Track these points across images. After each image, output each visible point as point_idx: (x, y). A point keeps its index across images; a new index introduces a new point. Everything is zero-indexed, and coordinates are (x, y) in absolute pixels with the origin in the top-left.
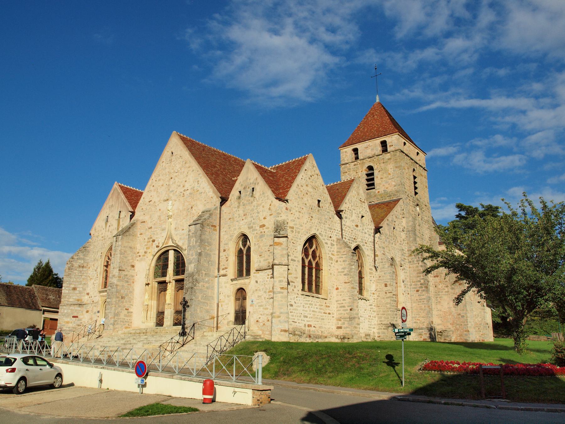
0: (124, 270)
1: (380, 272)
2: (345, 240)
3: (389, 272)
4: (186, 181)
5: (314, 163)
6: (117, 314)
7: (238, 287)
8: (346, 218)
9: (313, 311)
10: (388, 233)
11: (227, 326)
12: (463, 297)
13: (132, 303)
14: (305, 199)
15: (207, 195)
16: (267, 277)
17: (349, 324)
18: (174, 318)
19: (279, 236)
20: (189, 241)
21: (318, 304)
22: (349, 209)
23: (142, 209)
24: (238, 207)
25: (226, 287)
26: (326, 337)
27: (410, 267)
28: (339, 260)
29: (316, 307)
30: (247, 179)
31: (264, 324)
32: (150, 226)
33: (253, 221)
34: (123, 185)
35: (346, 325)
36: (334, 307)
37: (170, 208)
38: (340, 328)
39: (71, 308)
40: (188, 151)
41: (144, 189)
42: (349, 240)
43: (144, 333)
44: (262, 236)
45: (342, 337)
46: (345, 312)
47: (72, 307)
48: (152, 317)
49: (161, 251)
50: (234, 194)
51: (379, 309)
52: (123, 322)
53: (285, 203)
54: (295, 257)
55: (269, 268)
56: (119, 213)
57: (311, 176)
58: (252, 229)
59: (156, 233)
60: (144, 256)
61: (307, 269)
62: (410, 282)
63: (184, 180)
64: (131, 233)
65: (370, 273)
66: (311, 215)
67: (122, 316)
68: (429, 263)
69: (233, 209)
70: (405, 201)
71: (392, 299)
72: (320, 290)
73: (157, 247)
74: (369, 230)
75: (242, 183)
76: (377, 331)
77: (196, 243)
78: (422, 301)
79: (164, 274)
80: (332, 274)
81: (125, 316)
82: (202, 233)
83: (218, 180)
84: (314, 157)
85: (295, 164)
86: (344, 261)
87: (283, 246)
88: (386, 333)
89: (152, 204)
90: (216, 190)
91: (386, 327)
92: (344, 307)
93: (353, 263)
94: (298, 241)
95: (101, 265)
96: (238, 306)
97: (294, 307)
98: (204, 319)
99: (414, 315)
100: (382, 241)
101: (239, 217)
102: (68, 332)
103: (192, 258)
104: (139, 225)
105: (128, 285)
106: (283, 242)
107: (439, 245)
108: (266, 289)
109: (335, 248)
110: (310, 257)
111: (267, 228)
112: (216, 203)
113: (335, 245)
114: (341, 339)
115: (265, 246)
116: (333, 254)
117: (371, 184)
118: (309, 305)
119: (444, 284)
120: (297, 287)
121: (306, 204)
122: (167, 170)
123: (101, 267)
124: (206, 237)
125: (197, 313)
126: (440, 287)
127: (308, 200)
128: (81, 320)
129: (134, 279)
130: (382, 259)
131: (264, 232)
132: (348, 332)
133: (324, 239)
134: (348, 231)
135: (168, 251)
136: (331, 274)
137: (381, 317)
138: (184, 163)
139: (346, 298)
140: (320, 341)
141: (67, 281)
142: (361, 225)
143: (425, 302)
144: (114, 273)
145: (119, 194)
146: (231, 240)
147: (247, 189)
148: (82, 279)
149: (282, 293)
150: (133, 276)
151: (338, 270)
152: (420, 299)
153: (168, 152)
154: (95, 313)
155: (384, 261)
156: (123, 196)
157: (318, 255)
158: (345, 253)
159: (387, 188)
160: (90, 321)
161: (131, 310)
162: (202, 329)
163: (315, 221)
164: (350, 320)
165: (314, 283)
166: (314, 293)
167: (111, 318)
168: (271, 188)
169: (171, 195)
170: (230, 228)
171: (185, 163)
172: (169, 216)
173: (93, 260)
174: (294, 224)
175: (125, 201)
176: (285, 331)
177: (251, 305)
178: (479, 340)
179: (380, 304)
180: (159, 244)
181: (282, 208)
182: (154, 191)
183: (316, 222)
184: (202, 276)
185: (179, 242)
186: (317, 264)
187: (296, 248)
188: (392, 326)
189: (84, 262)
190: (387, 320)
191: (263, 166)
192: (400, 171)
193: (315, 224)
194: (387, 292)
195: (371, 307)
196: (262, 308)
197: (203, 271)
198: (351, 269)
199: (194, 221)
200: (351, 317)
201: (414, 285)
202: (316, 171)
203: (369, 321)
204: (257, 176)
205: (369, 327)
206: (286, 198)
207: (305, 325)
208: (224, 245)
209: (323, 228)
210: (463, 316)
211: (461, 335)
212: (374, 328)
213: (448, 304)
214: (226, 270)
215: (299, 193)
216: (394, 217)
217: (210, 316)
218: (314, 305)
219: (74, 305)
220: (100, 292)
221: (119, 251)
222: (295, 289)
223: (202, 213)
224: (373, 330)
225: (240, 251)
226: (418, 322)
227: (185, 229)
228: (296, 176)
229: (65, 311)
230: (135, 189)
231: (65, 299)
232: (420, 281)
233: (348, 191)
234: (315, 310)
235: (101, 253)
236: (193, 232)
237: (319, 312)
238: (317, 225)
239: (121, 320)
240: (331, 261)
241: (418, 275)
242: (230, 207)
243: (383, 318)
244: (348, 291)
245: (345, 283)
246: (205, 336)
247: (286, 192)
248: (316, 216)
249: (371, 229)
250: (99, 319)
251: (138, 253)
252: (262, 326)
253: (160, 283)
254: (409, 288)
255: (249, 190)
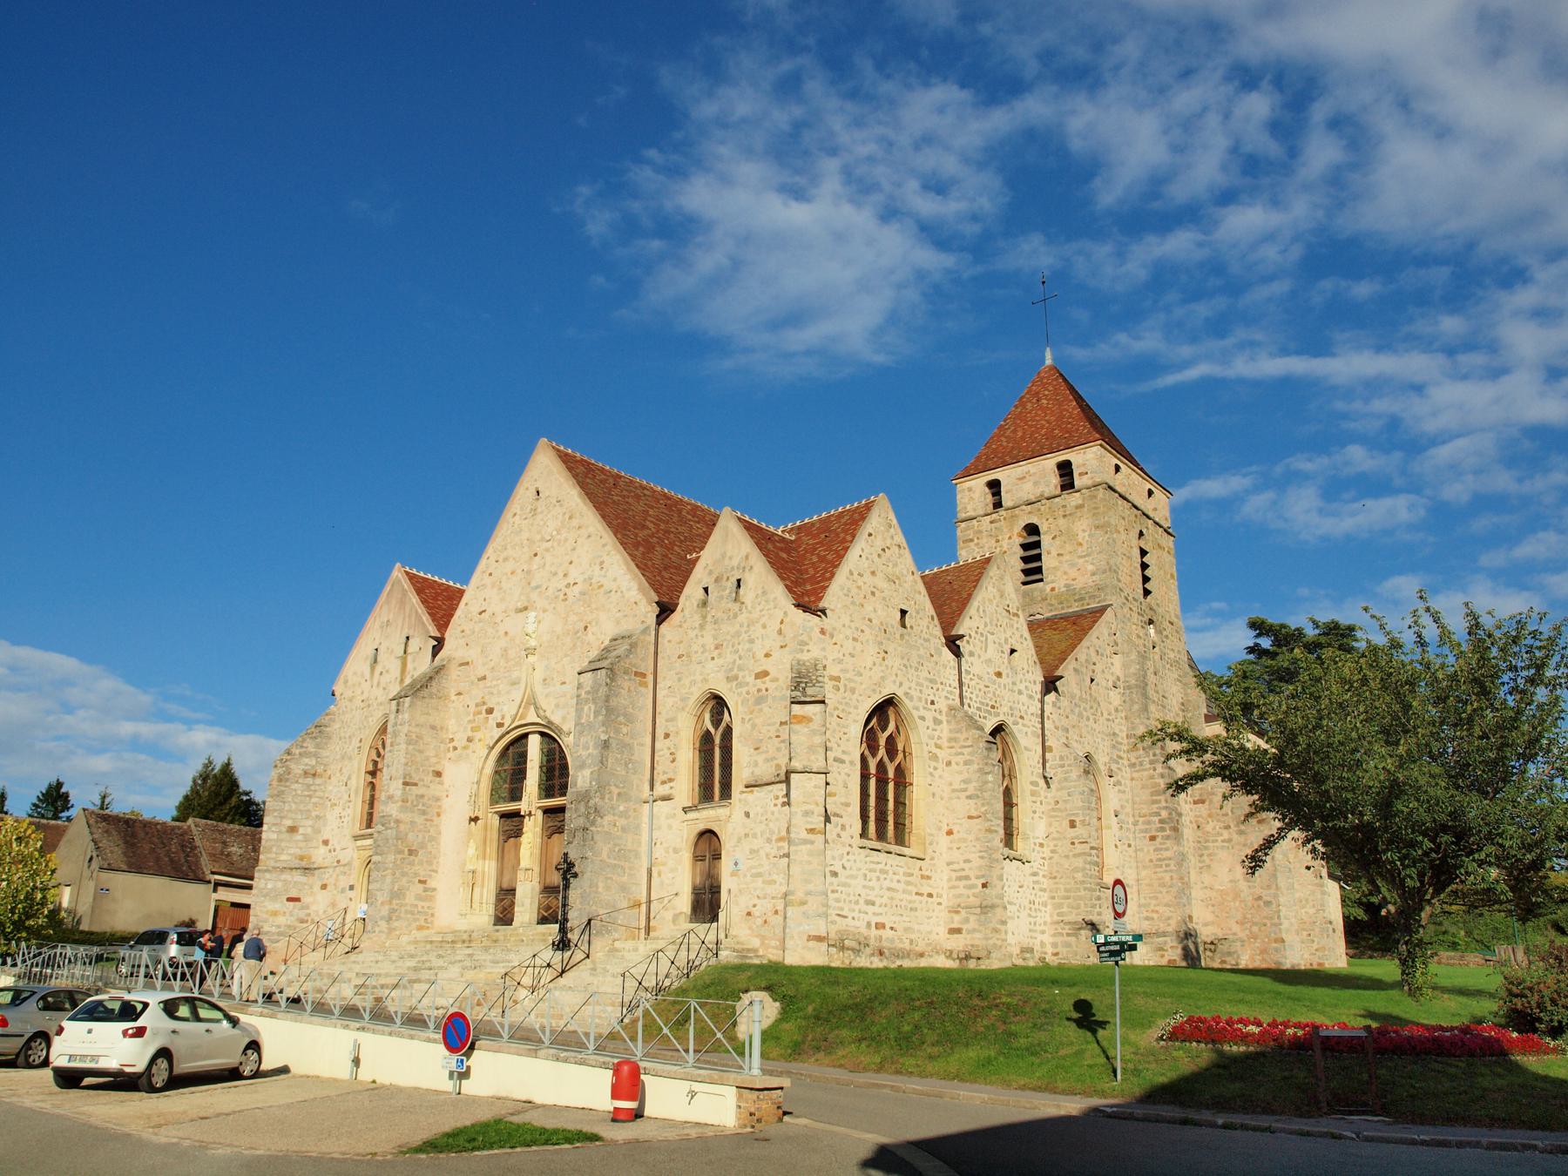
0: (416, 784)
1: (1058, 790)
2: (970, 711)
3: (1080, 790)
4: (571, 563)
5: (892, 516)
6: (397, 895)
7: (702, 827)
8: (971, 654)
9: (889, 889)
10: (1076, 691)
11: (672, 927)
12: (1266, 854)
13: (434, 867)
14: (869, 608)
15: (623, 597)
16: (774, 802)
17: (979, 920)
18: (540, 904)
19: (803, 699)
20: (579, 711)
21: (901, 871)
22: (980, 631)
23: (463, 631)
24: (702, 627)
25: (670, 827)
26: (922, 955)
27: (1132, 779)
28: (954, 760)
29: (897, 877)
30: (723, 556)
31: (765, 922)
32: (480, 674)
33: (738, 662)
34: (414, 571)
35: (972, 924)
36: (941, 880)
37: (530, 628)
38: (958, 931)
39: (283, 877)
40: (578, 488)
41: (466, 581)
42: (979, 709)
43: (464, 942)
44: (760, 700)
45: (962, 955)
46: (970, 892)
47: (286, 876)
48: (484, 901)
49: (508, 736)
50: (690, 595)
51: (1056, 883)
52: (413, 914)
53: (819, 616)
54: (844, 752)
55: (778, 779)
56: (404, 640)
57: (884, 550)
58: (735, 683)
59: (495, 692)
60: (465, 748)
61: (873, 782)
62: (1133, 816)
63: (568, 558)
64: (434, 690)
65: (1033, 794)
66: (883, 647)
67: (410, 898)
68: (1181, 768)
69: (690, 631)
70: (1119, 611)
71: (1089, 859)
72: (907, 835)
73: (500, 725)
74: (1027, 684)
75: (710, 567)
76: (1051, 940)
77: (595, 717)
78: (1164, 863)
79: (516, 795)
80: (937, 796)
81: (419, 897)
82: (610, 690)
83: (651, 560)
84: (892, 503)
85: (843, 521)
86: (966, 763)
87: (815, 725)
88: (1074, 944)
90: (647, 585)
91: (1074, 929)
92: (967, 878)
93: (988, 769)
94: (850, 713)
95: (359, 769)
96: (701, 875)
97: (841, 878)
98: (614, 906)
99: (1145, 898)
100: (1061, 711)
101: (702, 653)
102: (276, 937)
103: (584, 753)
104: (454, 672)
105: (427, 820)
106: (815, 715)
107: (1207, 722)
108: (772, 832)
109: (945, 730)
110: (882, 752)
111: (772, 681)
112: (646, 617)
113: (945, 722)
114: (961, 960)
115: (769, 725)
116: (937, 746)
117: (1032, 569)
118: (878, 874)
119: (1219, 821)
120: (847, 827)
121: (870, 620)
122: (525, 535)
123: (358, 777)
124: (621, 701)
125: (597, 892)
126: (1209, 828)
127: (875, 611)
128: (307, 907)
129: (440, 807)
130: (1061, 758)
131: (767, 690)
132: (977, 942)
133: (917, 709)
134: (978, 687)
135: (525, 736)
136: (934, 795)
137: (1060, 906)
138: (567, 516)
139: (971, 857)
140: (907, 963)
141: (275, 810)
142: (1009, 671)
143: (1172, 867)
144: (391, 792)
145: (404, 593)
146: (683, 709)
147: (724, 583)
148: (310, 807)
149: (812, 843)
150: (438, 799)
151: (951, 784)
152: (1160, 860)
153: (527, 489)
154: (343, 891)
155: (1066, 763)
156: (414, 599)
157: (900, 747)
158: (969, 743)
159: (1074, 580)
160: (330, 911)
161: (432, 884)
162: (609, 932)
163: (894, 662)
164: (982, 913)
165: (891, 819)
166: (890, 843)
167: (382, 903)
168: (782, 579)
169: (534, 596)
170: (679, 680)
171: (570, 518)
172: (528, 649)
173: (338, 757)
174: (842, 670)
175: (420, 611)
176: (819, 939)
177: (734, 874)
178: (1311, 965)
179: (1057, 872)
180: (503, 718)
181: (812, 629)
182: (493, 587)
183: (896, 664)
184: (611, 799)
185: (553, 712)
186: (900, 771)
187: (846, 731)
188: (1089, 927)
189: (317, 762)
190: (1075, 911)
191: (764, 526)
192: (1107, 536)
193: (895, 669)
194: (1076, 841)
195: (1035, 878)
196: (760, 879)
197: (613, 788)
198: (986, 782)
199: (590, 662)
200: (984, 903)
201: (1144, 823)
202: (896, 538)
203: (1030, 915)
204: (748, 550)
205: (1030, 931)
206: (821, 605)
207: (869, 924)
208: (667, 721)
209: (914, 678)
210: (1268, 903)
211: (1263, 951)
212: (1043, 932)
213: (1230, 871)
214: (671, 784)
215: (854, 591)
216: (1092, 651)
217: (629, 899)
218: (891, 872)
219: (291, 869)
220: (357, 838)
221: (404, 736)
222: (843, 834)
223: (611, 641)
224: (1040, 937)
225: (707, 738)
226: (1155, 916)
227: (567, 682)
228: (846, 549)
229: (269, 886)
230: (444, 581)
231: (269, 856)
232: (1158, 814)
233: (975, 587)
234: (894, 885)
235: (361, 741)
236: (589, 689)
237: (904, 892)
238: (899, 672)
239: (409, 908)
240: (933, 764)
241: (1154, 798)
242: (681, 626)
243: (1065, 906)
244: (978, 839)
245: (970, 817)
246: (617, 950)
247: (819, 592)
248: (895, 649)
249: (1035, 682)
250: (352, 905)
251: (452, 740)
252: (762, 926)
253: (504, 816)
254: (1133, 830)
255: (729, 584)
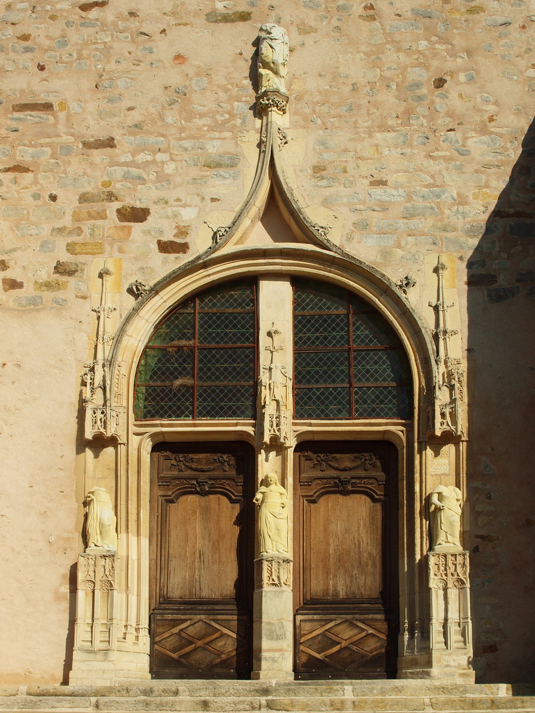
49: (202, 273)
60: (48, 285)
89: (110, 18)
